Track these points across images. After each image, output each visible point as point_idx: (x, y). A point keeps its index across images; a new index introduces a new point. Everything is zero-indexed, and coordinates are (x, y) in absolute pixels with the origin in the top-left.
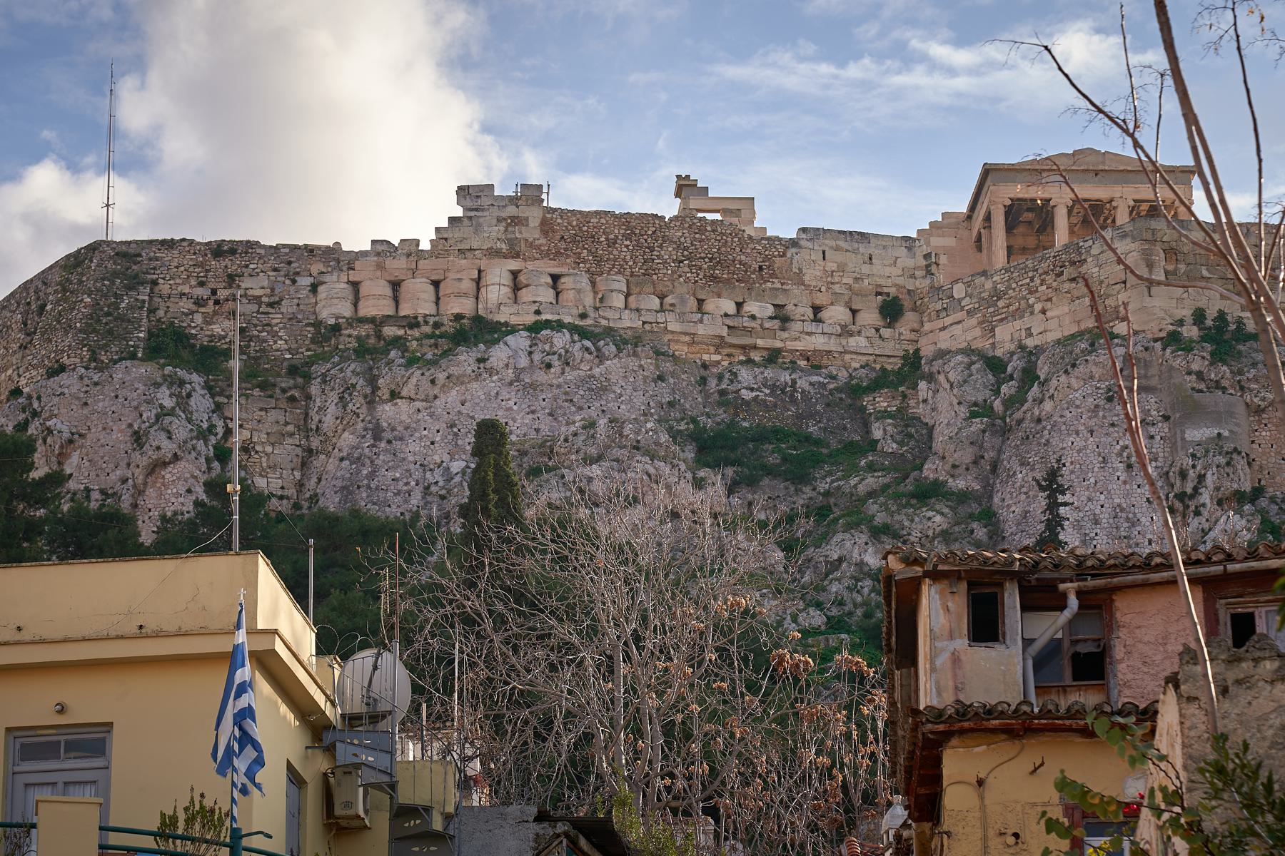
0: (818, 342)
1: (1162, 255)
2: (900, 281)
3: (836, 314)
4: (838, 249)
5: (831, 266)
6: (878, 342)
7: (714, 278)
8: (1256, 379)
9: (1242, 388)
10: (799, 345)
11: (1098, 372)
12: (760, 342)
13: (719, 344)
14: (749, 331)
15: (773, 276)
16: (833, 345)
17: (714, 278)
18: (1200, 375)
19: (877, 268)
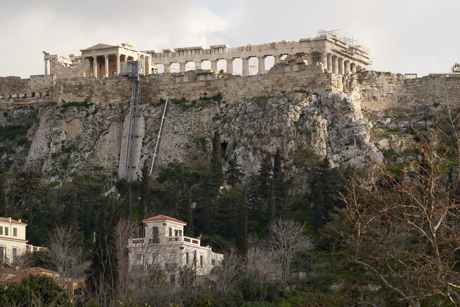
0: (33, 101)
1: (62, 87)
2: (50, 85)
3: (37, 94)
4: (37, 79)
5: (36, 84)
6: (44, 100)
7: (13, 90)
8: (68, 116)
9: (65, 118)
10: (28, 103)
11: (47, 115)
12: (21, 103)
13: (13, 105)
14: (19, 101)
15: (25, 88)
16: (35, 102)
17: (13, 90)
18: (59, 116)
19: (46, 83)
